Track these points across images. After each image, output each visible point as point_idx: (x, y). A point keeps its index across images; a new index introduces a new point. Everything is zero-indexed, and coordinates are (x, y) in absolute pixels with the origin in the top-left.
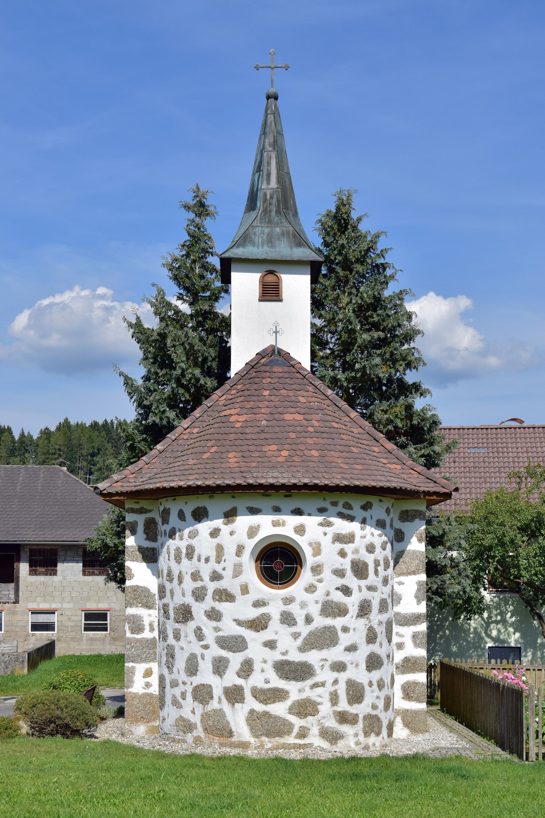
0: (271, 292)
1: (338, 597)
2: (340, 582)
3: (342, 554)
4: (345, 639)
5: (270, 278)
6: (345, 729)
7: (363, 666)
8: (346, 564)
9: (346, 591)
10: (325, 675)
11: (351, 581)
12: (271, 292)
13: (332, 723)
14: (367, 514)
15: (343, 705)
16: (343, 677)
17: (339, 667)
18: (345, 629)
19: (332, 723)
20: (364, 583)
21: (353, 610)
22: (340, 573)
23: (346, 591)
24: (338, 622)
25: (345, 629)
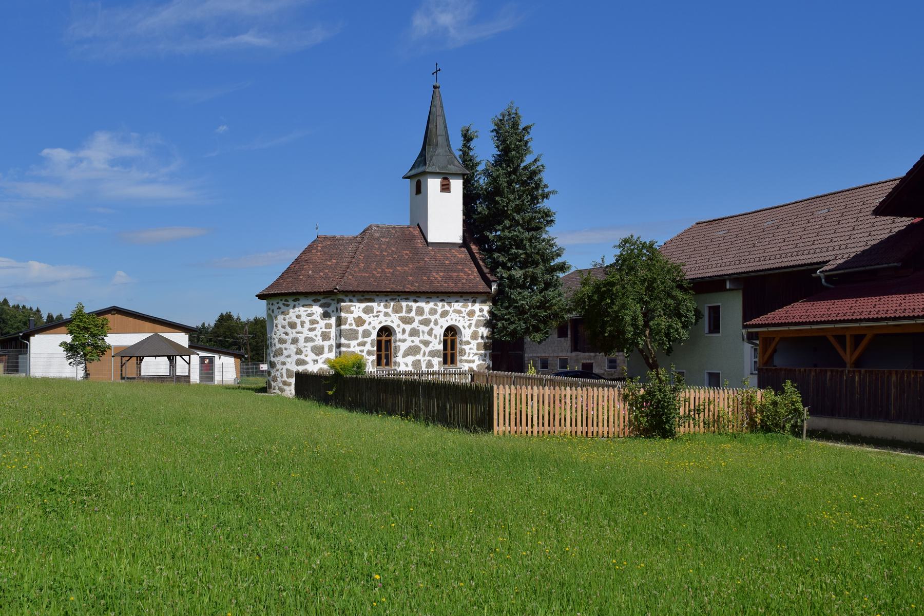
0: (445, 188)
1: (284, 336)
2: (284, 330)
3: (284, 319)
4: (285, 353)
5: (446, 182)
6: (285, 387)
7: (294, 363)
8: (286, 323)
9: (286, 334)
10: (279, 367)
11: (288, 330)
12: (445, 188)
13: (281, 385)
14: (296, 303)
15: (285, 378)
16: (285, 367)
17: (284, 364)
18: (286, 349)
19: (281, 385)
20: (294, 331)
21: (289, 341)
22: (284, 327)
23: (286, 334)
24: (283, 346)
25: (286, 349)
